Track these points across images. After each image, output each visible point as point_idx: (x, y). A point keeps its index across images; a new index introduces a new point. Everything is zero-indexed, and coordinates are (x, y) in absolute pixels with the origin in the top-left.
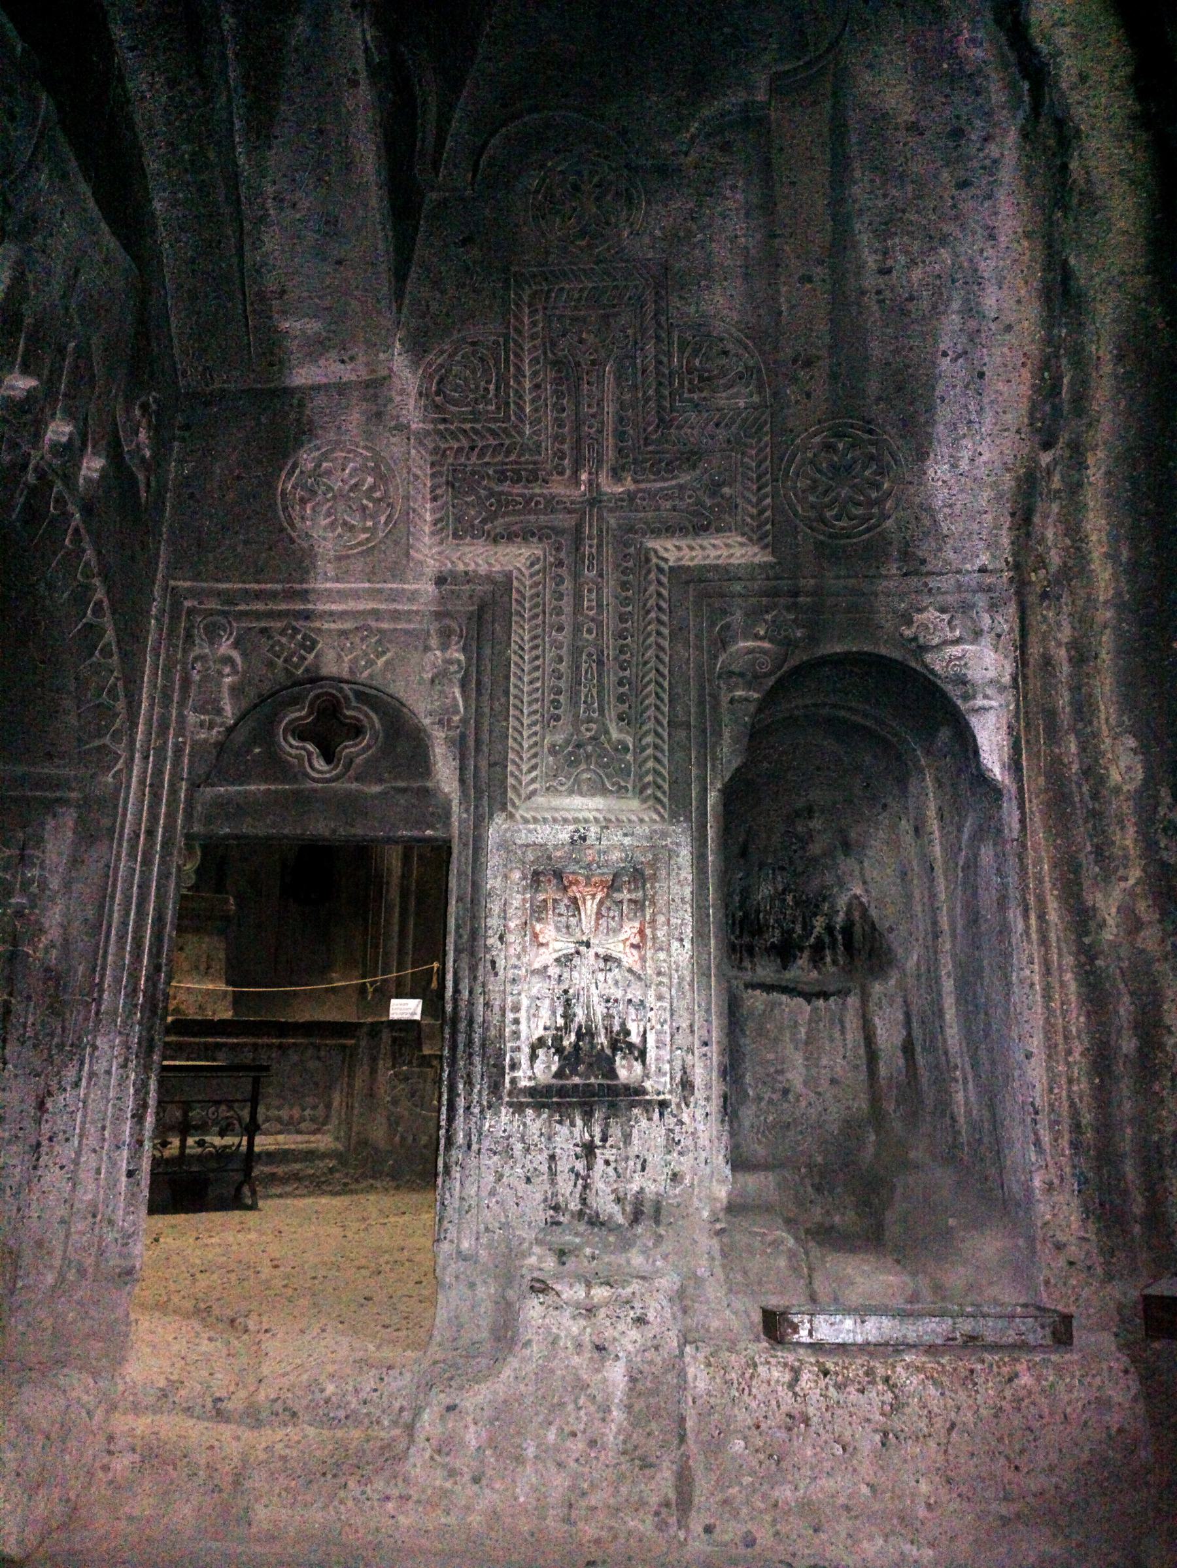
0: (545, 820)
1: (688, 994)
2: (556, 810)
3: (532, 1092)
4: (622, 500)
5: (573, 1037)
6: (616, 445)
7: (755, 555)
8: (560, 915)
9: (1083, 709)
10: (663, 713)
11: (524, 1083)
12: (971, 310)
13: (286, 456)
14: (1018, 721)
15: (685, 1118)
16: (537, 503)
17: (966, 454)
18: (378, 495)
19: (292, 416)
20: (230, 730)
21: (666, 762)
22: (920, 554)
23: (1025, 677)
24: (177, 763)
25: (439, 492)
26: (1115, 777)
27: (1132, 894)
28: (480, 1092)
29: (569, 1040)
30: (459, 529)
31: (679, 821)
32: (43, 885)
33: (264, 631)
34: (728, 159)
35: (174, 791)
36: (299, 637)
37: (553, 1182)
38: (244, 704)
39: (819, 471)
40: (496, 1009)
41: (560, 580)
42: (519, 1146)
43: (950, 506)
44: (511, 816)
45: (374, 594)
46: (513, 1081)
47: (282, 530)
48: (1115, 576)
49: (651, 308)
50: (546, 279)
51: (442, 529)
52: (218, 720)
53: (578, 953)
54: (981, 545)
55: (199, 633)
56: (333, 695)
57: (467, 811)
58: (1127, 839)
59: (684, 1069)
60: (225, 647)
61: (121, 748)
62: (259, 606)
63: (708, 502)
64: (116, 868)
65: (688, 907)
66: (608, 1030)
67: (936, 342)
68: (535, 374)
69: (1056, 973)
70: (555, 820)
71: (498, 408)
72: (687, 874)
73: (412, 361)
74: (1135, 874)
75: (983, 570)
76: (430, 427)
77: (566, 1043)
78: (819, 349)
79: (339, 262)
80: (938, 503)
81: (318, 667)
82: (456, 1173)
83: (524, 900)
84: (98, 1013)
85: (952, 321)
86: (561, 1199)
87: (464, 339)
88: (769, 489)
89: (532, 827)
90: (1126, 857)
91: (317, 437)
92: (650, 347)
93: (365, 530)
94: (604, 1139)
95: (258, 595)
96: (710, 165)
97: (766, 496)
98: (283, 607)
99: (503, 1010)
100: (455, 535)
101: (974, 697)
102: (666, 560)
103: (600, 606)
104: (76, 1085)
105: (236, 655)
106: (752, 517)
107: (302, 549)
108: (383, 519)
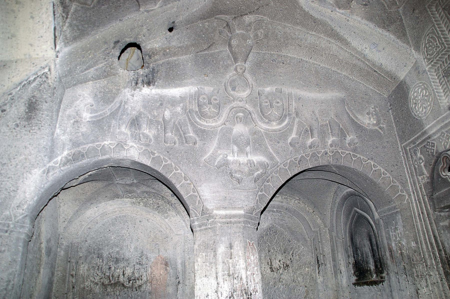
13: (408, 98)
18: (427, 94)
20: (432, 177)
33: (424, 146)
35: (424, 200)
45: (438, 122)
51: (447, 92)
52: (425, 176)
55: (413, 154)
56: (446, 156)
60: (419, 155)
61: (404, 193)
76: (430, 66)
79: (384, 49)
84: (426, 266)
93: (429, 106)
95: (418, 138)
98: (424, 138)
108: (431, 99)
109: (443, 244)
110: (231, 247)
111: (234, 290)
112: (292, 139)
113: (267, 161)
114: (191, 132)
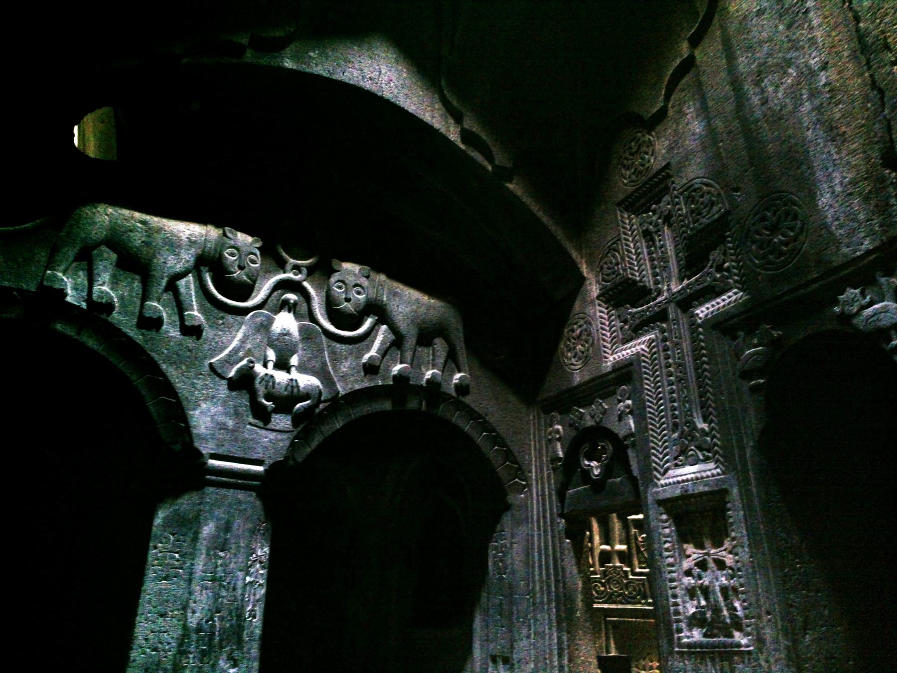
1: (752, 581)
3: (689, 645)
24: (549, 484)
29: (708, 615)
32: (505, 547)
39: (761, 235)
43: (837, 219)
44: (656, 485)
46: (679, 639)
63: (718, 276)
64: (533, 536)
75: (868, 252)
80: (829, 220)
83: (671, 531)
84: (534, 604)
99: (667, 595)
102: (701, 318)
104: (528, 637)
105: (560, 427)
110: (227, 528)
111: (217, 608)
112: (371, 358)
113: (321, 387)
114: (195, 307)
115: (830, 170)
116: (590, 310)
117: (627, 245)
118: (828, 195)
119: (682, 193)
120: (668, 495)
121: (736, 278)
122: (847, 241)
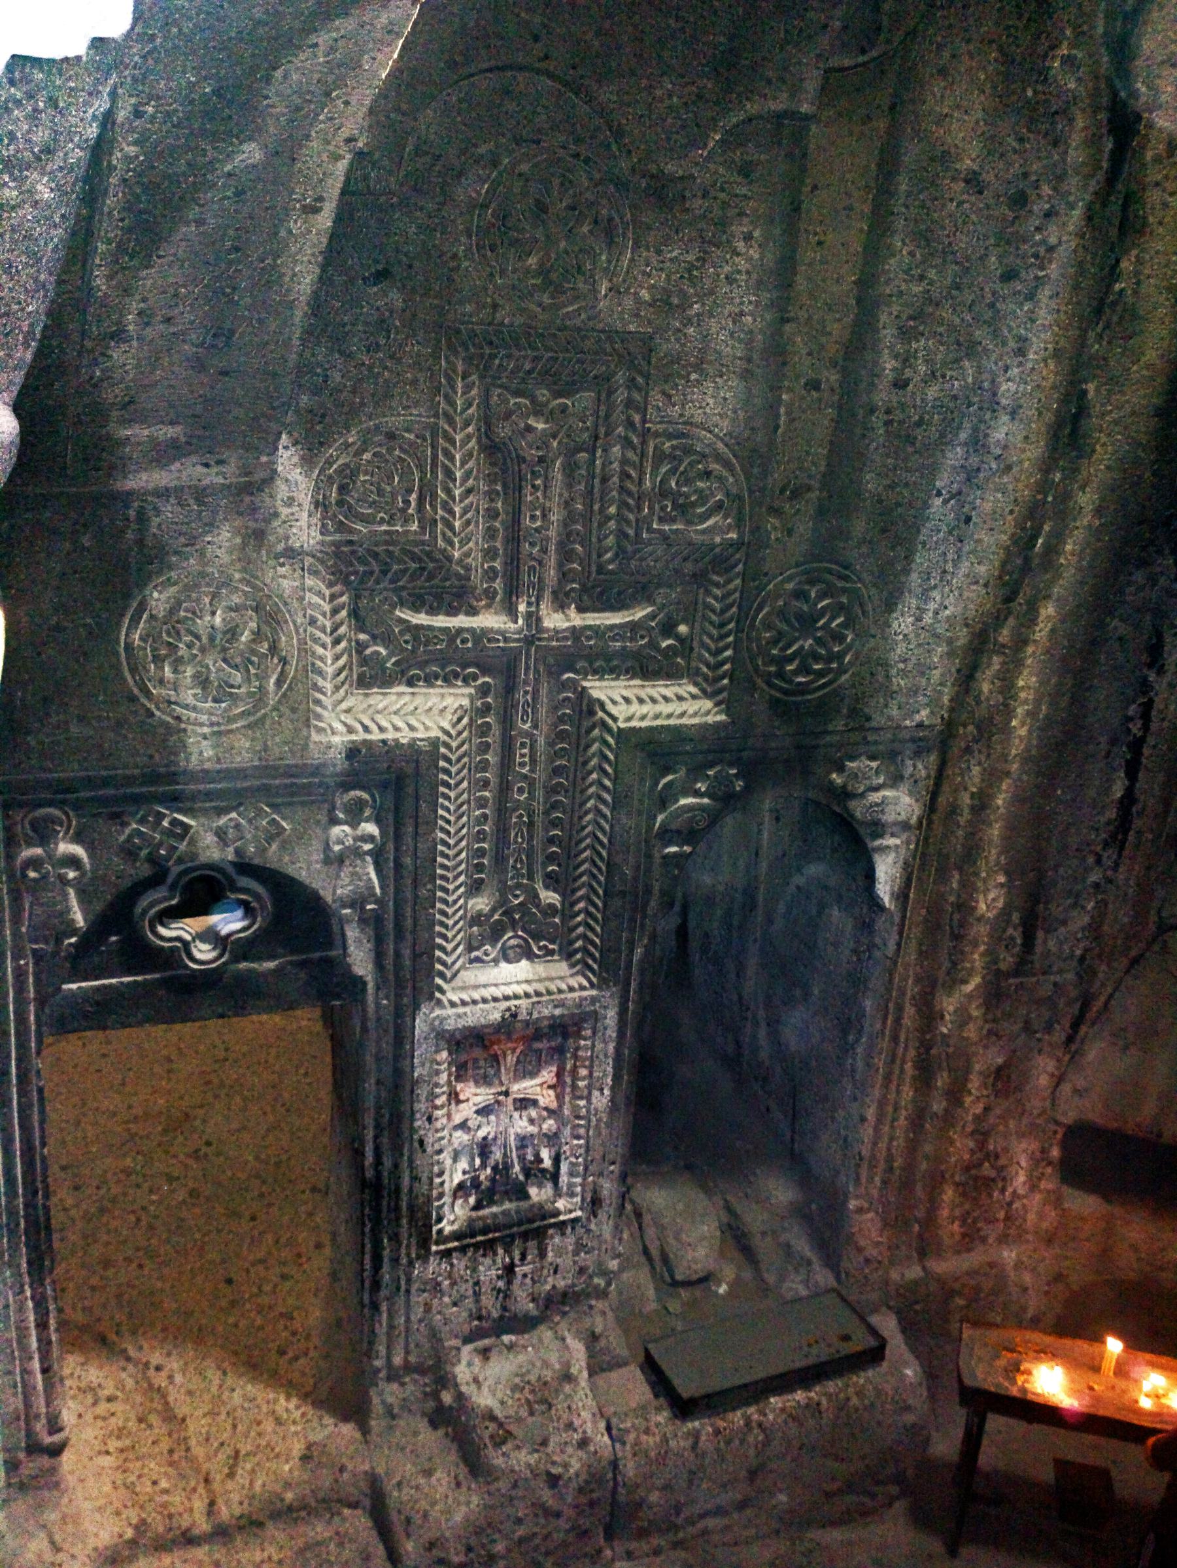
0: (474, 1002)
2: (485, 986)
3: (456, 1236)
4: (566, 638)
5: (489, 1170)
6: (560, 565)
7: (708, 713)
8: (479, 1068)
9: (972, 851)
10: (599, 883)
11: (448, 1229)
12: (977, 443)
13: (127, 596)
14: (914, 858)
15: (593, 1227)
16: (464, 641)
17: (932, 606)
19: (130, 535)
21: (598, 929)
22: (866, 710)
23: (930, 822)
24: (20, 989)
25: (343, 630)
26: (983, 906)
27: (970, 997)
28: (408, 1246)
30: (370, 676)
31: (608, 987)
34: (744, 191)
36: (165, 823)
37: (477, 1301)
38: (98, 907)
39: (788, 622)
40: (424, 1179)
41: (485, 730)
42: (447, 1283)
43: (905, 661)
44: (439, 1002)
46: (440, 1231)
47: (133, 699)
48: (1030, 732)
49: (621, 395)
50: (491, 343)
53: (498, 1102)
54: (924, 700)
57: (387, 998)
58: (977, 959)
59: (595, 1192)
60: (66, 847)
62: (111, 792)
65: (610, 1061)
66: (522, 1158)
67: (934, 480)
68: (467, 476)
69: (898, 1062)
70: (485, 1001)
71: (422, 528)
72: (612, 1033)
73: (302, 458)
74: (975, 981)
75: (920, 725)
77: (482, 1177)
78: (810, 477)
79: (225, 373)
80: (894, 656)
81: (194, 856)
82: (384, 1307)
85: (955, 456)
86: (484, 1312)
87: (377, 427)
88: (731, 639)
89: (461, 1010)
90: (972, 968)
91: (170, 568)
92: (616, 450)
94: (523, 1257)
96: (723, 195)
97: (726, 648)
100: (364, 682)
101: (881, 836)
102: (615, 719)
103: (533, 761)
105: (79, 850)
106: (708, 666)
107: (166, 725)
108: (272, 681)
109: (45, 1168)
115: (933, 582)
116: (285, 581)
117: (447, 453)
118: (910, 620)
119: (657, 435)
120: (470, 1021)
121: (705, 670)
122: (904, 700)
